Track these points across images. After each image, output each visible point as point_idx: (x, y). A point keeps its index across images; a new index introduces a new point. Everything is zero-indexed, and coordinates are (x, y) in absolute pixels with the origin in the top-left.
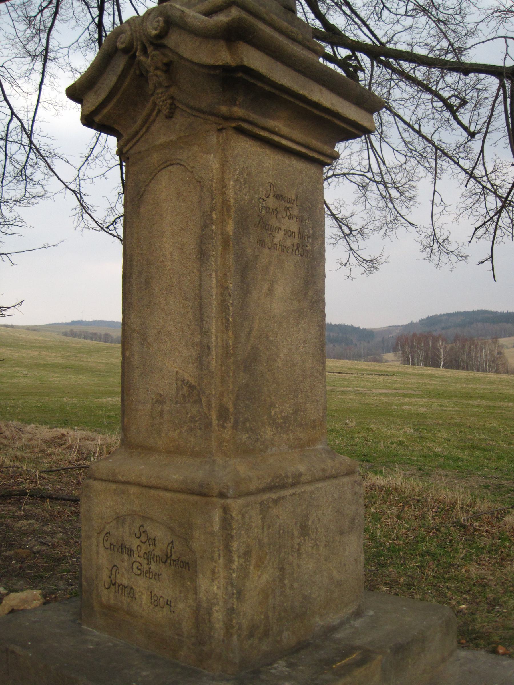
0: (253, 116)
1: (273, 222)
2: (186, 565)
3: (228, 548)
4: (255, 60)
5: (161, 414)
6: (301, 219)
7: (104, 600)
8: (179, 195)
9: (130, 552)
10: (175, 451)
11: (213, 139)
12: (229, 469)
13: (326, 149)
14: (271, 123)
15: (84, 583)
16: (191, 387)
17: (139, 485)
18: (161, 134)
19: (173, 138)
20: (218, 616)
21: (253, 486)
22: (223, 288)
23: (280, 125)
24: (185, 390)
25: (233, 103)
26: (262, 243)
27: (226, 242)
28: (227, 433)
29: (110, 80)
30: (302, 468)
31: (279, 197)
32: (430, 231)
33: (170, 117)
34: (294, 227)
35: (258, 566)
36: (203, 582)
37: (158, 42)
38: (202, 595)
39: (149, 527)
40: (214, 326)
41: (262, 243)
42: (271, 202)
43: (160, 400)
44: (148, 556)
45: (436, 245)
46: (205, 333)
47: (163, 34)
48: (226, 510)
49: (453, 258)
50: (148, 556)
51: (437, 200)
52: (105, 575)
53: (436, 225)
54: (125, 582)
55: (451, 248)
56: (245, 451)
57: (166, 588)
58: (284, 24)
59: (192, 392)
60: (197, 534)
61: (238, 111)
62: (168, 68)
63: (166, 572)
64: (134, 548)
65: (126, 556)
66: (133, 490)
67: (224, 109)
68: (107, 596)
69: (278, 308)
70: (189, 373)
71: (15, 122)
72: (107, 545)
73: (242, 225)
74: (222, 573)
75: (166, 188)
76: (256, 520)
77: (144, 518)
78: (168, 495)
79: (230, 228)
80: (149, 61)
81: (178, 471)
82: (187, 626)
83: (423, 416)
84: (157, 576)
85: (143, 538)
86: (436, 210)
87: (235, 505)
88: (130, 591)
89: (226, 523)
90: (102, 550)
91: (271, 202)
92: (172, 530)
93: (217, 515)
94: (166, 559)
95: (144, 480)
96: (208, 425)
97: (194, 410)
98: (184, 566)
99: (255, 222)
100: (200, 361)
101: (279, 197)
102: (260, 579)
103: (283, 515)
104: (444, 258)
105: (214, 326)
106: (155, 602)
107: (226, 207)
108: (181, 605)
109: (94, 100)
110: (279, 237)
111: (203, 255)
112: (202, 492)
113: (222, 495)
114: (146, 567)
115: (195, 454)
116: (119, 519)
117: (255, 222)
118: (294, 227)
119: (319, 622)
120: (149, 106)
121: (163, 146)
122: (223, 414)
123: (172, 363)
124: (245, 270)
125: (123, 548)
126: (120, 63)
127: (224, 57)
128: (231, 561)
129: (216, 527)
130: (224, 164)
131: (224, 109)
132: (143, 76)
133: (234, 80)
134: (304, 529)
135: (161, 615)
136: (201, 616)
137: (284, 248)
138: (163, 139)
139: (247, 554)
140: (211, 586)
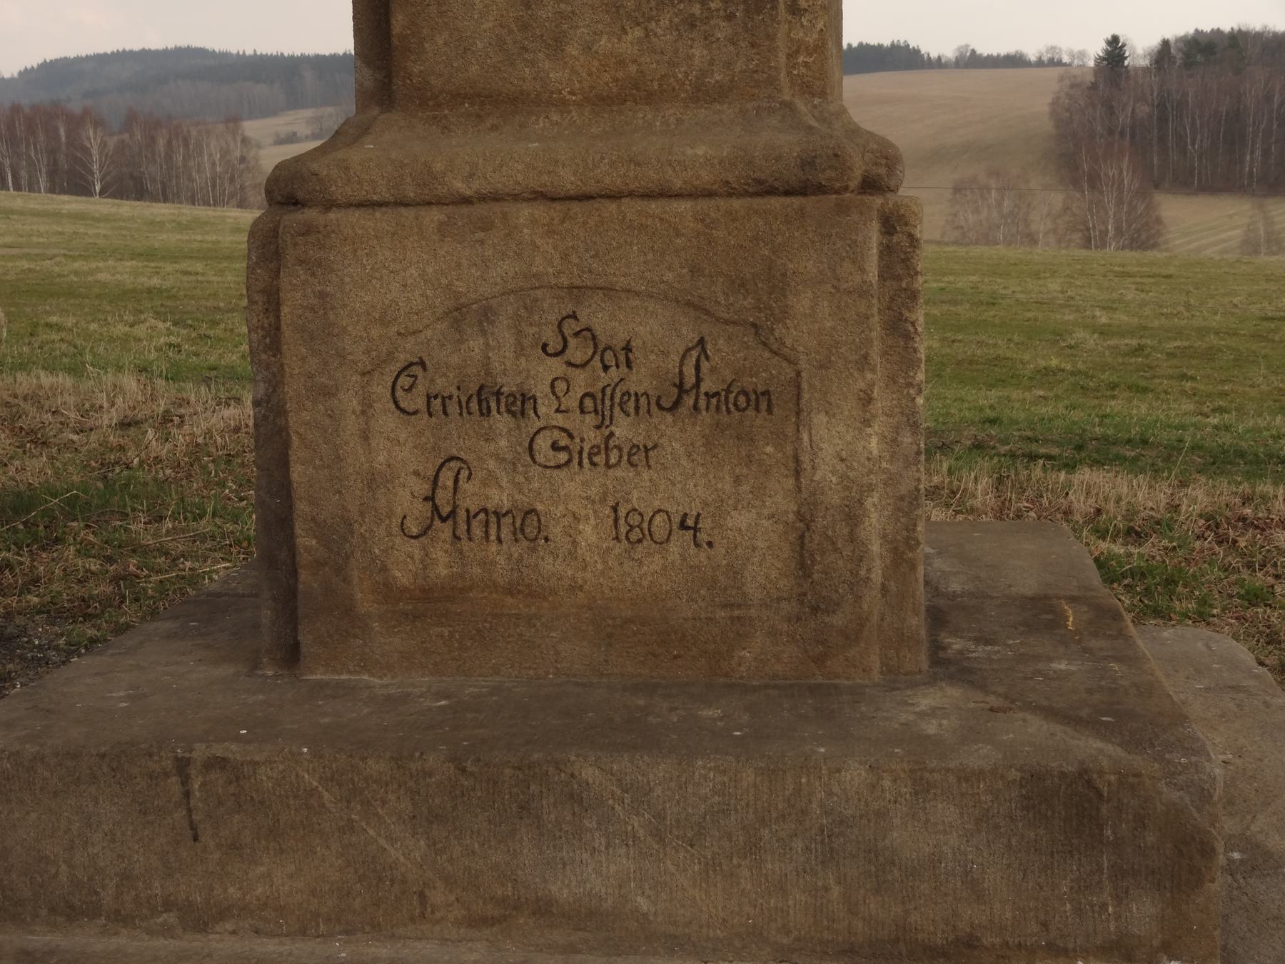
2: (761, 399)
3: (898, 328)
7: (401, 576)
9: (521, 404)
10: (624, 95)
15: (305, 540)
38: (825, 473)
39: (599, 316)
44: (599, 405)
50: (599, 405)
52: (407, 499)
54: (499, 498)
60: (801, 302)
63: (674, 436)
64: (541, 389)
65: (501, 422)
66: (524, 212)
68: (405, 563)
72: (416, 401)
74: (883, 400)
77: (577, 291)
78: (683, 206)
82: (766, 570)
84: (640, 454)
85: (577, 352)
88: (527, 524)
90: (387, 421)
92: (697, 308)
94: (678, 396)
95: (568, 180)
98: (749, 405)
106: (631, 529)
108: (740, 519)
114: (593, 437)
115: (703, 94)
125: (484, 398)
129: (873, 274)
135: (661, 566)
136: (811, 540)
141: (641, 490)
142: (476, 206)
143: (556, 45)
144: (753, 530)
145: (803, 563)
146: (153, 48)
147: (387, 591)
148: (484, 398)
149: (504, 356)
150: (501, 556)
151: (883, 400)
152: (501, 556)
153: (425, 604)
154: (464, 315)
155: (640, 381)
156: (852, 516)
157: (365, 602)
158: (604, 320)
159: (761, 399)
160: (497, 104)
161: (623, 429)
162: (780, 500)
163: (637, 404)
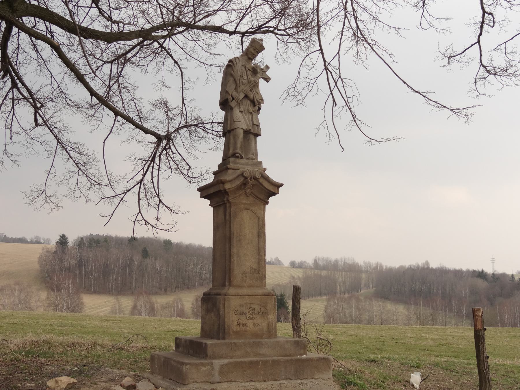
2: (265, 313)
5: (246, 277)
7: (234, 330)
8: (250, 219)
9: (246, 314)
10: (251, 286)
15: (226, 327)
16: (255, 270)
19: (248, 202)
24: (253, 270)
38: (270, 320)
43: (245, 273)
44: (252, 314)
50: (252, 314)
52: (236, 323)
54: (244, 322)
57: (259, 320)
60: (268, 305)
63: (258, 317)
65: (244, 315)
70: (255, 266)
82: (265, 329)
84: (255, 318)
86: (51, 176)
88: (246, 325)
90: (234, 315)
92: (260, 305)
94: (259, 313)
95: (250, 294)
97: (257, 275)
106: (254, 325)
108: (264, 324)
115: (257, 287)
121: (244, 204)
125: (243, 313)
138: (244, 202)
142: (242, 296)
143: (245, 282)
144: (264, 325)
145: (268, 328)
147: (233, 332)
148: (243, 313)
150: (243, 328)
152: (243, 328)
153: (236, 333)
154: (241, 306)
155: (256, 312)
156: (272, 324)
157: (231, 333)
158: (253, 306)
159: (265, 313)
160: (240, 287)
161: (254, 316)
162: (267, 322)
163: (255, 314)
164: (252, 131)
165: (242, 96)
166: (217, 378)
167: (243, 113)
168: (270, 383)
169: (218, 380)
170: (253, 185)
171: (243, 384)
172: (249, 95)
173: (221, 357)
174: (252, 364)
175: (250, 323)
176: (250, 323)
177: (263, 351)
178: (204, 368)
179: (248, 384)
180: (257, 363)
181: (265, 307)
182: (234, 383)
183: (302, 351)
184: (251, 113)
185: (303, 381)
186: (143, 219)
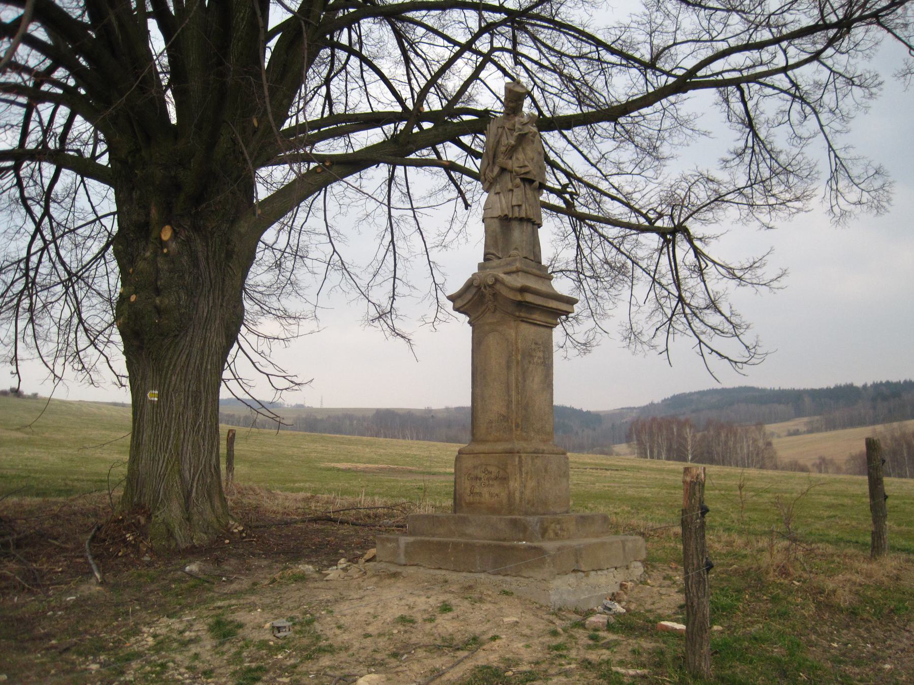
0: (527, 315)
1: (534, 354)
2: (505, 479)
3: (520, 470)
4: (529, 298)
6: (544, 352)
9: (480, 479)
11: (513, 324)
12: (518, 445)
13: (554, 322)
14: (534, 316)
16: (504, 416)
17: (484, 453)
18: (489, 318)
20: (517, 495)
21: (529, 450)
22: (517, 379)
23: (537, 317)
25: (520, 311)
26: (530, 362)
27: (518, 363)
28: (519, 432)
29: (469, 296)
30: (545, 448)
31: (536, 344)
32: (628, 326)
33: (494, 312)
34: (541, 354)
35: (531, 478)
36: (511, 483)
37: (491, 286)
38: (511, 488)
40: (513, 393)
41: (530, 362)
42: (533, 346)
43: (491, 422)
44: (488, 479)
45: (633, 337)
46: (510, 396)
47: (494, 284)
48: (520, 457)
49: (646, 347)
50: (488, 479)
51: (634, 301)
52: (468, 491)
53: (633, 321)
55: (643, 340)
56: (525, 440)
57: (496, 489)
58: (538, 272)
59: (505, 418)
60: (509, 467)
61: (523, 315)
62: (494, 295)
63: (496, 483)
67: (517, 314)
68: (469, 499)
69: (535, 387)
70: (503, 411)
71: (336, 256)
73: (523, 357)
74: (518, 479)
75: (492, 340)
76: (530, 462)
79: (519, 358)
80: (487, 292)
81: (500, 447)
82: (505, 501)
83: (646, 499)
84: (492, 486)
86: (633, 309)
87: (523, 456)
88: (480, 494)
89: (520, 461)
91: (533, 346)
92: (498, 467)
93: (517, 459)
94: (496, 478)
95: (486, 451)
96: (512, 430)
98: (503, 479)
99: (528, 354)
100: (508, 407)
101: (536, 344)
102: (531, 484)
103: (538, 462)
104: (639, 346)
105: (513, 393)
106: (491, 495)
107: (517, 348)
109: (460, 303)
110: (536, 359)
111: (509, 368)
112: (511, 452)
113: (518, 452)
116: (475, 467)
117: (528, 354)
118: (541, 354)
119: (552, 509)
120: (484, 307)
121: (491, 323)
122: (517, 426)
123: (496, 407)
124: (524, 373)
125: (477, 478)
126: (474, 291)
127: (519, 298)
128: (521, 475)
130: (516, 333)
131: (517, 314)
132: (483, 296)
133: (522, 305)
134: (546, 471)
136: (510, 496)
137: (538, 364)
139: (527, 473)
140: (514, 484)
141: (493, 490)
144: (504, 495)
145: (509, 500)
146: (658, 400)
149: (478, 472)
150: (477, 498)
151: (518, 479)
152: (477, 498)
158: (490, 469)
159: (505, 479)
160: (484, 441)
161: (491, 482)
162: (507, 492)
163: (492, 479)
164: (510, 216)
165: (496, 170)
166: (402, 559)
167: (501, 195)
168: (464, 574)
169: (403, 562)
170: (494, 295)
171: (432, 571)
172: (504, 166)
173: (411, 534)
174: (442, 547)
175: (485, 491)
176: (485, 491)
177: (470, 530)
178: (389, 545)
179: (438, 572)
180: (446, 545)
181: (504, 470)
182: (422, 569)
183: (521, 535)
184: (512, 190)
185: (508, 578)
186: (712, 350)
